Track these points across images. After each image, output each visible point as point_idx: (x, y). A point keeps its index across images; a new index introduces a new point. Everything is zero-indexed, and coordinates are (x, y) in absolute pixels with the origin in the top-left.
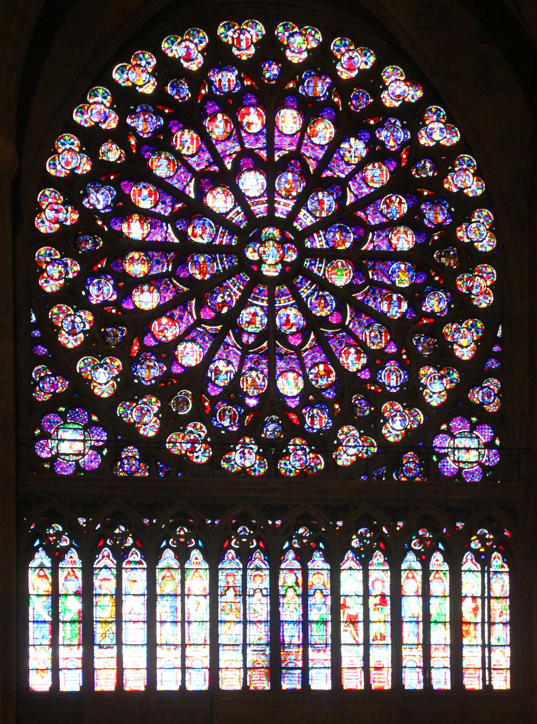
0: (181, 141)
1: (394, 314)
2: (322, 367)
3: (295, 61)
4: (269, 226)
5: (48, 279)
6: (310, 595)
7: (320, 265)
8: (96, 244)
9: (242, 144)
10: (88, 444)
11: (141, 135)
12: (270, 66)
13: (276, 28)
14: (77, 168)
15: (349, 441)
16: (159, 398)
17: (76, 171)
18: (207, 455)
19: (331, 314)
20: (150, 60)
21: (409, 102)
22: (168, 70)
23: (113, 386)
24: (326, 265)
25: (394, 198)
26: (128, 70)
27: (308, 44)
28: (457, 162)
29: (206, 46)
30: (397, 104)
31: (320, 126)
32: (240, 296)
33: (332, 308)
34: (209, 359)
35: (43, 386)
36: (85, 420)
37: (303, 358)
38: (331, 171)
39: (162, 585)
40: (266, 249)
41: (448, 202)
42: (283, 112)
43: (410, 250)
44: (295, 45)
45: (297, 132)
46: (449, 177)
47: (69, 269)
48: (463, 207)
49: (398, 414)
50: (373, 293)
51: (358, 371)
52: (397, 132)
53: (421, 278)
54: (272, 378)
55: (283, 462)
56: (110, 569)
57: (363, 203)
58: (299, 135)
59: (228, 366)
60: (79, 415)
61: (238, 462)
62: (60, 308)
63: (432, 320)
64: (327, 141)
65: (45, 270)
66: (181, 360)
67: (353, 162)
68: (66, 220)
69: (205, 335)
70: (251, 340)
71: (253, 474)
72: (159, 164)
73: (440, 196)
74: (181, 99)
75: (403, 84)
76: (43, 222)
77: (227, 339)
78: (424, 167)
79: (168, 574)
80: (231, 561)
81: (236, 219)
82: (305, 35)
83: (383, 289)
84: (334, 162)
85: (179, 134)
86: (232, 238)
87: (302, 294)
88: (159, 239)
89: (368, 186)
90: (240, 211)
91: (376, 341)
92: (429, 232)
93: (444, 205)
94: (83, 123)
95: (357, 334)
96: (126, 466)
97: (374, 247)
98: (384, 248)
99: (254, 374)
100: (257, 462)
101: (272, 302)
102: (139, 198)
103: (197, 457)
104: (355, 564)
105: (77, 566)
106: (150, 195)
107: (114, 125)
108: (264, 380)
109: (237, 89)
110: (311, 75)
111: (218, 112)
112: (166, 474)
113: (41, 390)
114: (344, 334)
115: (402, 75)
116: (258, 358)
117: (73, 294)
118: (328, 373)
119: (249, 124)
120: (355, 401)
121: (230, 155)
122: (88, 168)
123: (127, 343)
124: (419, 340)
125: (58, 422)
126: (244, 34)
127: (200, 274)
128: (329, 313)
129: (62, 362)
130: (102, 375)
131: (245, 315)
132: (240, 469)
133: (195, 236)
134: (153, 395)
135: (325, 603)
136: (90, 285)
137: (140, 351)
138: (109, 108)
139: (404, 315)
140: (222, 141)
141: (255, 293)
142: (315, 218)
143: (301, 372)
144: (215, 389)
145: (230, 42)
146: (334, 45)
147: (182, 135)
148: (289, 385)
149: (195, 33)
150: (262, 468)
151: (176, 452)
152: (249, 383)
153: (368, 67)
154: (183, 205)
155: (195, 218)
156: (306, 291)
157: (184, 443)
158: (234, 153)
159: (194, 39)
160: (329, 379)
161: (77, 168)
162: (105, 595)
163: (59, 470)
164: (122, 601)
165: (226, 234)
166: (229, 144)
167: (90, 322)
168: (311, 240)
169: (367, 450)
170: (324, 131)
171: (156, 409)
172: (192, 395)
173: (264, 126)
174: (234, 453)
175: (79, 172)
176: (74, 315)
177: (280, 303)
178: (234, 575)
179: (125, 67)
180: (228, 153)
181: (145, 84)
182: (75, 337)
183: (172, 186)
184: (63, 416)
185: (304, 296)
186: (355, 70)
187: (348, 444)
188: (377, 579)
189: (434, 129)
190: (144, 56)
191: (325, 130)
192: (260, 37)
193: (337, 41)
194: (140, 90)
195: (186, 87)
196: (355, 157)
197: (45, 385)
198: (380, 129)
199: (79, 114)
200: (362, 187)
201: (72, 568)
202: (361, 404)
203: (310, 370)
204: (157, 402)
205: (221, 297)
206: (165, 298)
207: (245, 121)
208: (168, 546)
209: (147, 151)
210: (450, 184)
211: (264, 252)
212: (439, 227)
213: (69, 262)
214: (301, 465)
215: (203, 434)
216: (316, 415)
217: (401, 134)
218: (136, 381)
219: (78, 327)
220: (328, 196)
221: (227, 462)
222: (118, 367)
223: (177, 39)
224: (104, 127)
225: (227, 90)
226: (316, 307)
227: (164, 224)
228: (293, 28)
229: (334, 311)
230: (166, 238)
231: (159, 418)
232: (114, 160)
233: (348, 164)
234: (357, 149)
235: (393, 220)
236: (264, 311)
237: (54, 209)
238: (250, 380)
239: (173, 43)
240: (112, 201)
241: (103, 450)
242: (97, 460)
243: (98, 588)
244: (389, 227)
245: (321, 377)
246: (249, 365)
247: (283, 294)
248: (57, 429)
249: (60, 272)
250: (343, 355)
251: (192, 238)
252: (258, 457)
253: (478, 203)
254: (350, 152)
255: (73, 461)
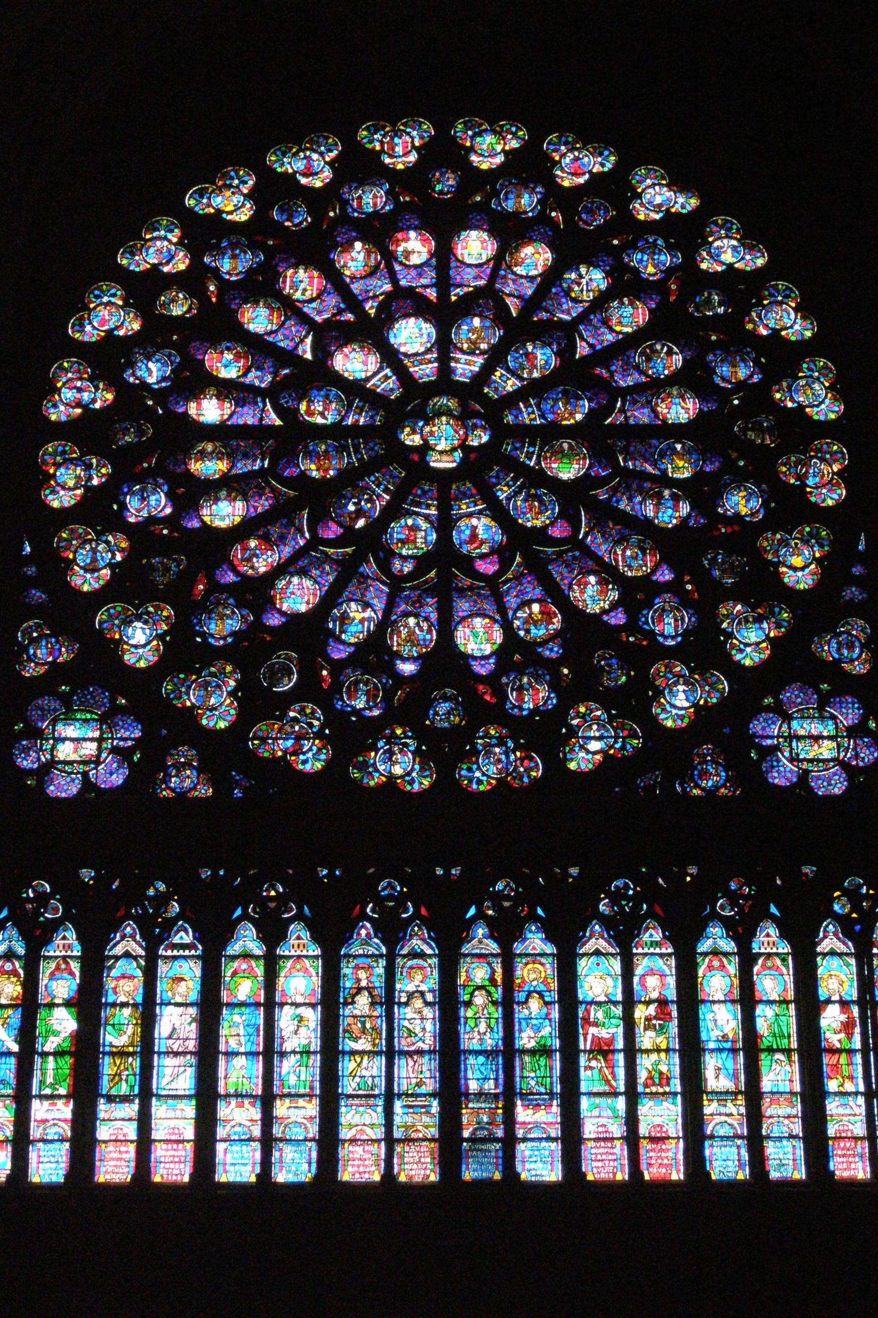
0: (292, 281)
1: (666, 519)
2: (536, 607)
3: (484, 167)
4: (440, 394)
5: (58, 488)
6: (519, 1003)
7: (531, 449)
8: (140, 432)
9: (394, 280)
10: (108, 745)
11: (227, 277)
12: (443, 174)
13: (452, 125)
14: (117, 328)
15: (590, 727)
16: (237, 666)
17: (116, 333)
18: (323, 757)
19: (552, 524)
20: (246, 178)
21: (678, 214)
22: (273, 190)
23: (158, 650)
24: (541, 449)
25: (658, 347)
26: (213, 191)
27: (505, 144)
28: (766, 293)
29: (337, 155)
30: (657, 217)
31: (528, 250)
32: (388, 502)
33: (553, 513)
34: (330, 600)
35: (35, 652)
36: (104, 705)
37: (502, 593)
38: (547, 311)
39: (232, 986)
40: (435, 429)
41: (753, 349)
42: (464, 234)
43: (691, 422)
44: (485, 147)
45: (488, 261)
46: (754, 314)
47: (93, 472)
48: (781, 359)
49: (681, 682)
50: (628, 488)
51: (604, 612)
52: (659, 254)
53: (712, 463)
54: (446, 626)
55: (465, 766)
56: (135, 958)
57: (605, 356)
58: (491, 264)
59: (364, 611)
60: (93, 698)
61: (381, 768)
62: (72, 531)
63: (736, 528)
64: (540, 269)
65: (54, 476)
66: (281, 603)
67: (585, 298)
68: (94, 401)
69: (324, 563)
70: (408, 568)
71: (409, 788)
72: (254, 315)
73: (738, 340)
74: (294, 225)
75: (665, 189)
76: (55, 406)
77: (365, 569)
78: (709, 302)
79: (244, 966)
80: (365, 941)
81: (383, 386)
82: (500, 134)
83: (646, 481)
84: (552, 299)
85: (291, 271)
86: (377, 414)
87: (499, 493)
88: (250, 422)
89: (611, 330)
90: (390, 374)
91: (635, 564)
92: (724, 395)
93: (748, 354)
94: (132, 268)
95: (600, 554)
96: (173, 780)
97: (626, 418)
98: (646, 420)
99: (412, 621)
100: (417, 767)
101: (445, 508)
102: (219, 365)
103: (305, 762)
104: (604, 943)
105: (75, 953)
106: (237, 357)
107: (182, 267)
108: (429, 631)
109: (387, 208)
110: (511, 183)
111: (356, 239)
112: (245, 791)
113: (30, 660)
114: (577, 553)
115: (663, 178)
116: (420, 596)
117: (98, 511)
118: (548, 616)
119: (407, 254)
120: (599, 662)
121: (375, 297)
122: (136, 326)
123: (187, 579)
124: (714, 559)
125: (55, 710)
126: (400, 138)
127: (318, 470)
128: (548, 522)
129: (71, 614)
130: (139, 632)
131: (397, 530)
132: (384, 779)
133: (310, 413)
134: (228, 661)
135: (547, 1017)
136: (126, 494)
137: (208, 592)
138: (175, 244)
139: (684, 521)
140: (361, 278)
141: (416, 495)
142: (521, 379)
143: (497, 617)
144: (341, 647)
145: (378, 148)
146: (549, 143)
147: (296, 273)
148: (477, 639)
149: (321, 140)
150: (425, 777)
151: (266, 755)
152: (403, 636)
153: (606, 169)
154: (291, 372)
155: (312, 389)
156: (505, 489)
157: (280, 738)
158: (381, 294)
159: (319, 147)
160: (550, 627)
161: (117, 328)
162: (124, 1005)
163: (52, 788)
164: (155, 1016)
165: (366, 408)
166: (373, 282)
167: (122, 550)
168: (514, 412)
169: (624, 743)
170: (535, 258)
171: (232, 683)
172: (300, 661)
173: (432, 255)
174: (373, 754)
175: (121, 333)
176: (96, 541)
177: (460, 509)
178: (370, 967)
179: (207, 188)
180: (371, 294)
181: (235, 210)
182: (96, 574)
183: (273, 345)
184: (66, 701)
185: (502, 496)
186: (584, 174)
187: (588, 734)
188: (651, 972)
189: (722, 248)
190: (237, 173)
191: (537, 256)
192: (427, 139)
193: (553, 137)
194: (229, 217)
195: (303, 209)
196: (588, 291)
197: (39, 652)
198: (629, 252)
199: (128, 256)
200: (603, 333)
201: (64, 958)
202: (610, 666)
203: (515, 612)
204: (234, 672)
205: (354, 504)
206: (256, 508)
207: (400, 249)
208: (245, 917)
209: (234, 299)
210: (755, 323)
211: (432, 433)
212: (741, 385)
213: (94, 461)
214: (500, 772)
215: (316, 723)
216: (526, 686)
217: (665, 259)
218: (199, 640)
219: (102, 558)
220: (543, 348)
221: (360, 770)
222: (168, 618)
223: (292, 148)
224: (166, 269)
225: (371, 210)
226: (525, 514)
227: (259, 399)
228: (481, 125)
229: (556, 519)
230: (262, 419)
231: (236, 698)
232: (180, 313)
233: (575, 301)
234: (591, 280)
235: (658, 378)
236: (431, 522)
237: (75, 387)
238: (404, 632)
239: (284, 154)
240: (172, 371)
241: (135, 753)
242: (121, 771)
243: (110, 992)
244: (650, 389)
245: (535, 623)
246: (403, 607)
247: (465, 496)
248: (54, 722)
249: (78, 477)
250: (575, 587)
251: (307, 418)
252: (418, 760)
253: (803, 350)
254: (579, 284)
255: (78, 773)
